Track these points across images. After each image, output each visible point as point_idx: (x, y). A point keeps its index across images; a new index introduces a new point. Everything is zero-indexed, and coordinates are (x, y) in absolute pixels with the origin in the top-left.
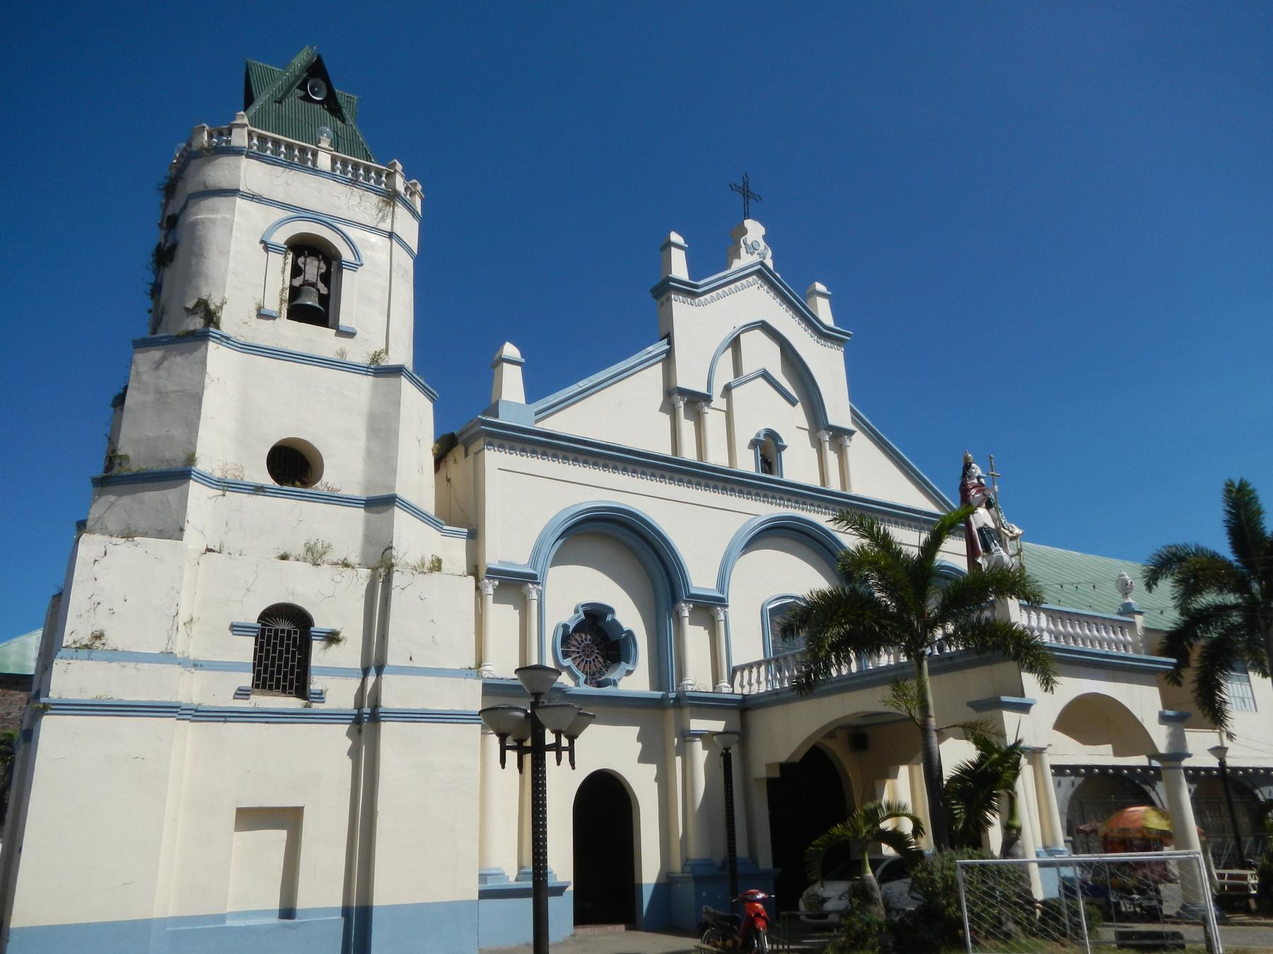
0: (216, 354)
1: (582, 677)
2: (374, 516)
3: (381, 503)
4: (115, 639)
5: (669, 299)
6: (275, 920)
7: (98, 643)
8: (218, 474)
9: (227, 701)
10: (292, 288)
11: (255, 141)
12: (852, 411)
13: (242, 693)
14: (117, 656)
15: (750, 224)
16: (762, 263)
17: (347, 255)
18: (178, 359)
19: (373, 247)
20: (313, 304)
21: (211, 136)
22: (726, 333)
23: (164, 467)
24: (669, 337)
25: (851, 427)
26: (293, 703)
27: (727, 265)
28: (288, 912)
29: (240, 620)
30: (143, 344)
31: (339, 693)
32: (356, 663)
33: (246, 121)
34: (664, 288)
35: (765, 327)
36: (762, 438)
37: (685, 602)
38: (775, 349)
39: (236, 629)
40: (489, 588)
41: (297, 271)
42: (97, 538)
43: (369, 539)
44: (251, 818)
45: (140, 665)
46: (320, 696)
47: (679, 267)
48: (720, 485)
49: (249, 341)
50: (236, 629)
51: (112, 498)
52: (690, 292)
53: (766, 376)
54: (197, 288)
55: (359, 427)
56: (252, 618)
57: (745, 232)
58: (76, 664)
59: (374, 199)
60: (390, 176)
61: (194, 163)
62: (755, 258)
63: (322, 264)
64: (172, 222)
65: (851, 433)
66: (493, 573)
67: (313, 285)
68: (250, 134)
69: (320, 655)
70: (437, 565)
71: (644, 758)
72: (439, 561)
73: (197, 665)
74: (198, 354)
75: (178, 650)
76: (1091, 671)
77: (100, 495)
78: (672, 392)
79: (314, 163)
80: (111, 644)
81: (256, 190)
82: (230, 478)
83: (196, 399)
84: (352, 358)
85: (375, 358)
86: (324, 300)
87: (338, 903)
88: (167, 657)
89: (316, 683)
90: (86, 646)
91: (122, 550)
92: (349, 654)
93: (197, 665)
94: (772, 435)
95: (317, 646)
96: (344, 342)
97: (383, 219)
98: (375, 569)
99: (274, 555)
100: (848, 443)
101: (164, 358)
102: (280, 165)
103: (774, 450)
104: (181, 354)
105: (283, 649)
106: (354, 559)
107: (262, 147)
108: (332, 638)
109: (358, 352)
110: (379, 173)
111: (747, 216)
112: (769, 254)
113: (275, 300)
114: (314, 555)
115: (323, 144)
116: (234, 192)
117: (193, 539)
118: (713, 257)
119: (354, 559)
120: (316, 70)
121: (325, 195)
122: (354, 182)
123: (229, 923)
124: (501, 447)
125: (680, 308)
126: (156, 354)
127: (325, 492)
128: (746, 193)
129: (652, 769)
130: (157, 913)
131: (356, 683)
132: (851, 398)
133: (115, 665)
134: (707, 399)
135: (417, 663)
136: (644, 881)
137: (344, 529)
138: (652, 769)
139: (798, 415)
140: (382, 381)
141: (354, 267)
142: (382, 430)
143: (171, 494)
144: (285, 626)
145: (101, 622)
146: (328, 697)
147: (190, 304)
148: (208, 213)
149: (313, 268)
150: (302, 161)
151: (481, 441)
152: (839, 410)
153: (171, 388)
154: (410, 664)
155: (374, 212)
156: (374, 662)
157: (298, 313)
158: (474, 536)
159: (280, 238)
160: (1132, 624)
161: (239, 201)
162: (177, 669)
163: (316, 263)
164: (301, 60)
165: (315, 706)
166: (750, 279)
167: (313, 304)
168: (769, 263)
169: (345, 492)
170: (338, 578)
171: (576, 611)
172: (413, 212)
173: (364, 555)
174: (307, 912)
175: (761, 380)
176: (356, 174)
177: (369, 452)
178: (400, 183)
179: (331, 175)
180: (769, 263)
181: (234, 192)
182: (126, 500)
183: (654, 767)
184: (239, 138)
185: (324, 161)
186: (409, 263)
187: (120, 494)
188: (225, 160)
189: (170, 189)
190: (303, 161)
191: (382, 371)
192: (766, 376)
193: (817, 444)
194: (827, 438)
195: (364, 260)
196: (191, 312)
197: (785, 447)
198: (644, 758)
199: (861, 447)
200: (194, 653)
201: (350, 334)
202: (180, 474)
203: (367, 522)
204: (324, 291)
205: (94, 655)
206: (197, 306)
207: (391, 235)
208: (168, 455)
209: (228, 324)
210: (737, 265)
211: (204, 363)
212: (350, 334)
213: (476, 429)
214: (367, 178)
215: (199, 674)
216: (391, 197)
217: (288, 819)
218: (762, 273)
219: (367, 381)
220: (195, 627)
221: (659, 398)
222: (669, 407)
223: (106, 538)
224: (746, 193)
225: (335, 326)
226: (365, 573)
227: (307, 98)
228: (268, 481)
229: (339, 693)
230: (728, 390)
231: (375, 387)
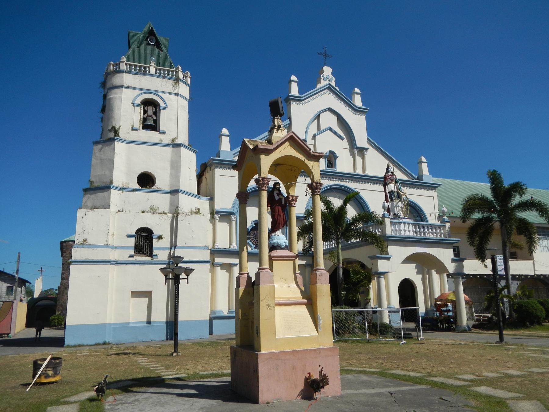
0: (118, 146)
1: (253, 246)
2: (173, 196)
3: (174, 192)
4: (90, 241)
5: (290, 103)
6: (145, 325)
7: (85, 243)
8: (121, 186)
9: (126, 259)
10: (144, 118)
12: (368, 139)
13: (131, 256)
14: (91, 246)
15: (325, 68)
16: (330, 84)
17: (162, 104)
18: (107, 148)
19: (171, 100)
20: (151, 124)
21: (114, 66)
22: (314, 114)
23: (104, 185)
24: (290, 118)
25: (367, 146)
26: (148, 259)
27: (316, 87)
28: (149, 322)
29: (130, 233)
30: (96, 143)
31: (162, 255)
32: (168, 245)
33: (125, 60)
34: (289, 99)
35: (331, 110)
36: (328, 154)
38: (335, 118)
39: (129, 236)
40: (217, 217)
41: (145, 112)
42: (83, 210)
43: (171, 204)
44: (136, 294)
45: (98, 249)
46: (156, 256)
47: (295, 90)
49: (129, 139)
51: (89, 195)
52: (298, 100)
53: (331, 129)
54: (112, 122)
55: (168, 166)
56: (134, 232)
57: (323, 72)
58: (79, 249)
59: (171, 82)
60: (177, 72)
61: (109, 77)
62: (328, 82)
63: (154, 109)
64: (105, 96)
66: (218, 212)
67: (151, 116)
68: (126, 64)
69: (156, 243)
70: (198, 212)
72: (199, 209)
73: (116, 248)
74: (112, 146)
75: (110, 243)
76: (421, 244)
77: (85, 194)
79: (149, 72)
80: (89, 243)
81: (129, 85)
82: (125, 187)
83: (112, 161)
84: (165, 142)
85: (173, 141)
86: (155, 121)
87: (164, 319)
88: (106, 246)
89: (155, 252)
90: (82, 244)
91: (90, 213)
92: (166, 242)
93: (116, 248)
94: (332, 153)
96: (162, 136)
97: (175, 89)
98: (173, 214)
99: (140, 211)
100: (366, 153)
101: (102, 148)
103: (333, 158)
104: (107, 146)
105: (144, 241)
106: (167, 211)
107: (131, 69)
108: (160, 237)
109: (167, 139)
110: (173, 72)
111: (325, 65)
112: (334, 79)
113: (138, 124)
114: (153, 211)
115: (153, 64)
117: (113, 208)
118: (309, 85)
119: (167, 211)
120: (151, 33)
121: (153, 83)
122: (164, 77)
123: (130, 325)
124: (221, 167)
125: (295, 107)
126: (100, 146)
127: (157, 189)
128: (325, 55)
130: (108, 322)
131: (168, 252)
132: (367, 135)
133: (90, 249)
135: (187, 245)
137: (163, 201)
139: (345, 143)
140: (175, 149)
141: (164, 108)
142: (175, 166)
143: (105, 194)
144: (145, 234)
145: (85, 236)
147: (110, 128)
148: (114, 95)
149: (150, 110)
150: (145, 72)
151: (214, 166)
152: (362, 140)
153: (105, 158)
154: (185, 245)
155: (171, 87)
156: (174, 245)
157: (146, 127)
158: (212, 199)
159: (138, 101)
160: (445, 226)
161: (124, 89)
162: (109, 250)
163: (151, 108)
164: (146, 30)
166: (325, 91)
167: (151, 124)
168: (333, 84)
169: (163, 189)
170: (161, 218)
171: (251, 223)
172: (187, 84)
173: (170, 209)
174: (155, 322)
176: (164, 74)
177: (171, 174)
178: (180, 75)
179: (155, 75)
180: (333, 84)
182: (93, 196)
184: (123, 67)
185: (153, 71)
186: (185, 104)
187: (91, 194)
188: (119, 75)
189: (104, 84)
190: (145, 71)
191: (175, 145)
192: (331, 129)
193: (353, 154)
194: (357, 152)
195: (168, 106)
196: (110, 131)
197: (337, 157)
199: (372, 155)
200: (116, 244)
201: (164, 133)
202: (107, 187)
203: (171, 198)
204: (155, 118)
205: (84, 246)
206: (112, 128)
207: (178, 95)
208: (105, 180)
209: (122, 134)
210: (319, 86)
211: (114, 149)
212: (164, 133)
213: (211, 162)
214: (168, 75)
215: (117, 250)
216: (177, 80)
217: (148, 294)
218: (330, 88)
219: (170, 149)
220: (115, 236)
223: (85, 210)
224: (325, 55)
225: (159, 131)
226: (170, 216)
227: (148, 44)
228: (138, 187)
229: (162, 255)
230: (314, 137)
231: (173, 151)
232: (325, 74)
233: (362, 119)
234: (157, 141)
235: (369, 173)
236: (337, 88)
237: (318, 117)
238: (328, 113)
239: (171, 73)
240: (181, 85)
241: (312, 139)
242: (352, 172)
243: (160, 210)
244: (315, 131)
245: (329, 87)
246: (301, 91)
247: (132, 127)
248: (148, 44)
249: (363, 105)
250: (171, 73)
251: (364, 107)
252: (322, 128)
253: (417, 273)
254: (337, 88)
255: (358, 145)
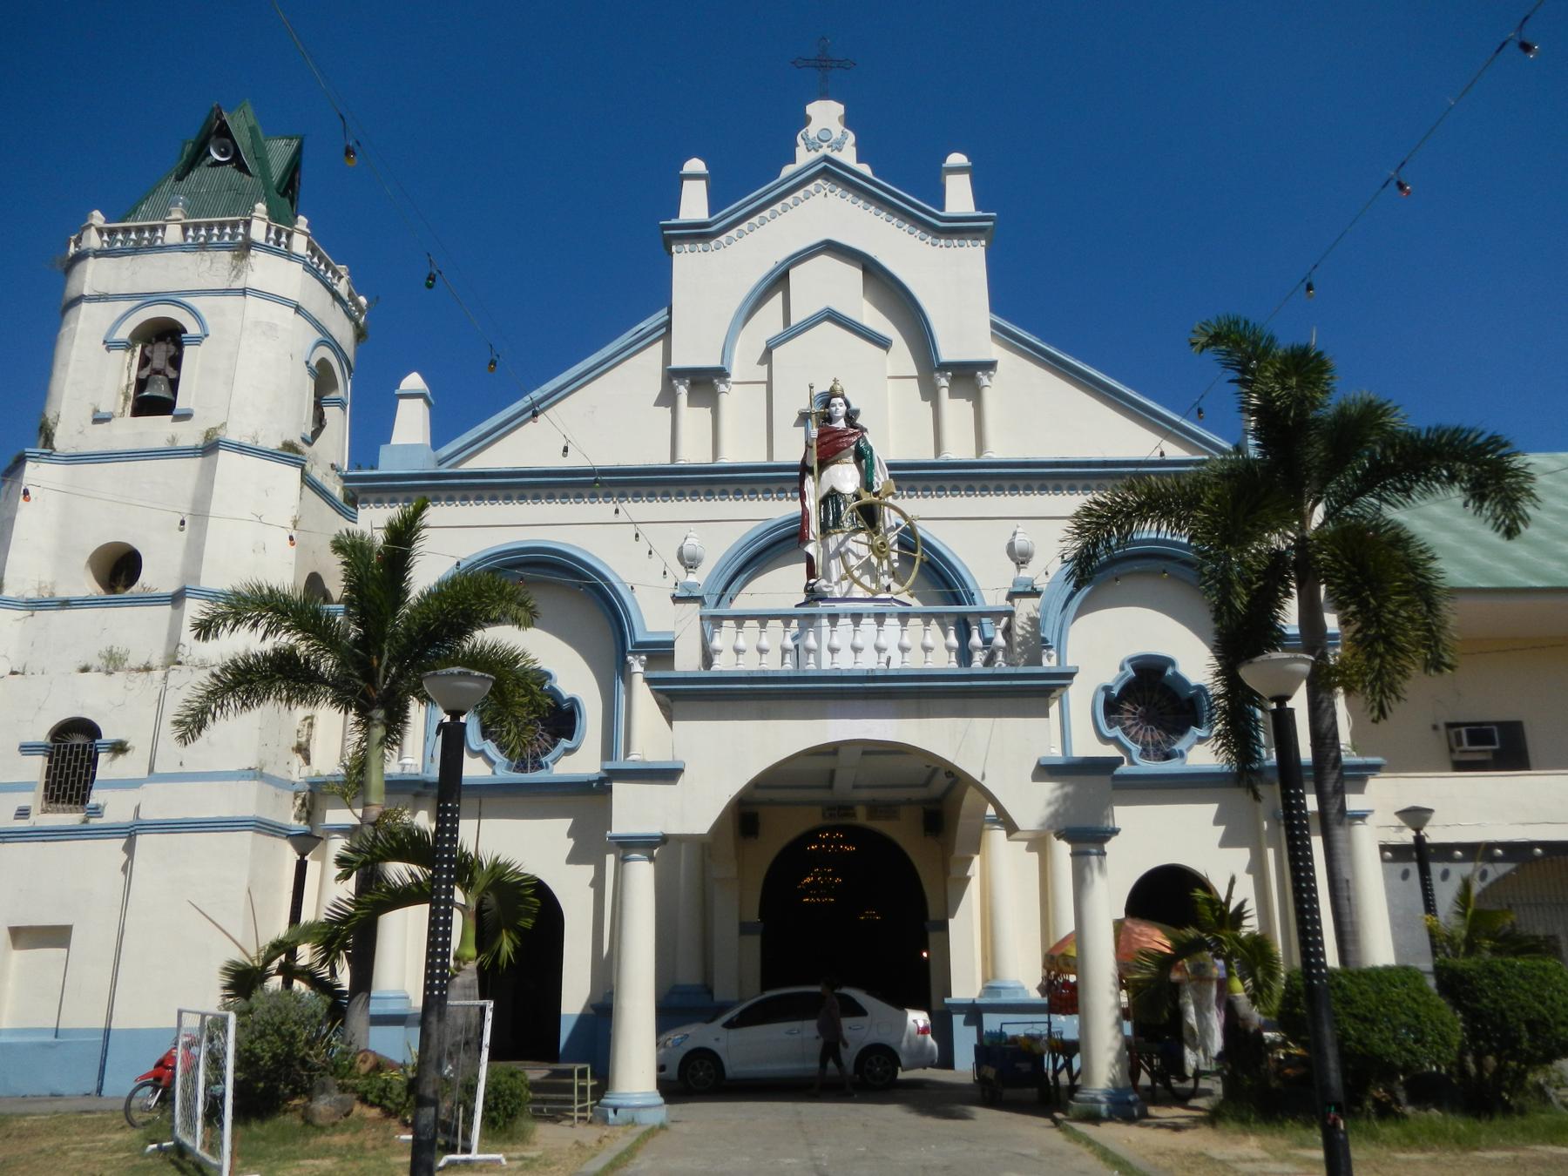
3: (177, 599)
5: (671, 254)
8: (32, 594)
11: (106, 238)
12: (994, 325)
13: (23, 813)
15: (813, 109)
16: (826, 158)
17: (192, 328)
25: (989, 349)
29: (29, 740)
37: (632, 653)
38: (855, 274)
39: (26, 749)
41: (145, 361)
44: (23, 936)
48: (702, 489)
49: (73, 451)
50: (26, 749)
52: (700, 234)
53: (832, 316)
56: (41, 735)
57: (805, 121)
60: (248, 224)
65: (989, 366)
68: (100, 231)
71: (575, 858)
78: (672, 375)
81: (102, 289)
84: (181, 444)
86: (174, 385)
89: (97, 797)
95: (103, 758)
96: (182, 426)
97: (237, 276)
100: (985, 380)
102: (127, 254)
108: (119, 748)
109: (189, 434)
111: (825, 96)
112: (851, 137)
114: (113, 662)
116: (80, 299)
118: (749, 178)
121: (172, 271)
122: (203, 247)
125: (686, 263)
129: (588, 871)
132: (994, 308)
134: (721, 373)
135: (187, 769)
136: (563, 1011)
138: (588, 871)
139: (901, 357)
141: (197, 340)
144: (79, 740)
146: (106, 812)
154: (181, 770)
159: (124, 333)
165: (92, 821)
166: (811, 187)
168: (848, 156)
170: (130, 685)
175: (827, 325)
178: (258, 231)
180: (848, 156)
181: (80, 299)
183: (592, 868)
185: (173, 234)
192: (832, 316)
193: (930, 393)
194: (944, 382)
198: (575, 858)
201: (186, 416)
204: (172, 375)
210: (788, 170)
212: (186, 416)
214: (220, 237)
218: (830, 172)
219: (194, 464)
221: (656, 386)
222: (667, 398)
232: (812, 130)
233: (972, 258)
234: (161, 443)
235: (1000, 449)
236: (865, 169)
237: (779, 281)
238: (824, 260)
239: (216, 231)
240: (258, 258)
241: (761, 362)
242: (928, 456)
243: (135, 660)
244: (777, 328)
245: (825, 169)
246: (715, 204)
247: (96, 411)
248: (217, 164)
249: (977, 208)
250: (216, 231)
251: (980, 213)
252: (795, 319)
253: (1226, 842)
254: (865, 169)
255: (948, 352)
